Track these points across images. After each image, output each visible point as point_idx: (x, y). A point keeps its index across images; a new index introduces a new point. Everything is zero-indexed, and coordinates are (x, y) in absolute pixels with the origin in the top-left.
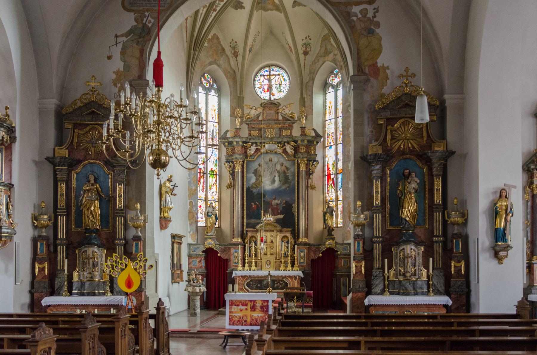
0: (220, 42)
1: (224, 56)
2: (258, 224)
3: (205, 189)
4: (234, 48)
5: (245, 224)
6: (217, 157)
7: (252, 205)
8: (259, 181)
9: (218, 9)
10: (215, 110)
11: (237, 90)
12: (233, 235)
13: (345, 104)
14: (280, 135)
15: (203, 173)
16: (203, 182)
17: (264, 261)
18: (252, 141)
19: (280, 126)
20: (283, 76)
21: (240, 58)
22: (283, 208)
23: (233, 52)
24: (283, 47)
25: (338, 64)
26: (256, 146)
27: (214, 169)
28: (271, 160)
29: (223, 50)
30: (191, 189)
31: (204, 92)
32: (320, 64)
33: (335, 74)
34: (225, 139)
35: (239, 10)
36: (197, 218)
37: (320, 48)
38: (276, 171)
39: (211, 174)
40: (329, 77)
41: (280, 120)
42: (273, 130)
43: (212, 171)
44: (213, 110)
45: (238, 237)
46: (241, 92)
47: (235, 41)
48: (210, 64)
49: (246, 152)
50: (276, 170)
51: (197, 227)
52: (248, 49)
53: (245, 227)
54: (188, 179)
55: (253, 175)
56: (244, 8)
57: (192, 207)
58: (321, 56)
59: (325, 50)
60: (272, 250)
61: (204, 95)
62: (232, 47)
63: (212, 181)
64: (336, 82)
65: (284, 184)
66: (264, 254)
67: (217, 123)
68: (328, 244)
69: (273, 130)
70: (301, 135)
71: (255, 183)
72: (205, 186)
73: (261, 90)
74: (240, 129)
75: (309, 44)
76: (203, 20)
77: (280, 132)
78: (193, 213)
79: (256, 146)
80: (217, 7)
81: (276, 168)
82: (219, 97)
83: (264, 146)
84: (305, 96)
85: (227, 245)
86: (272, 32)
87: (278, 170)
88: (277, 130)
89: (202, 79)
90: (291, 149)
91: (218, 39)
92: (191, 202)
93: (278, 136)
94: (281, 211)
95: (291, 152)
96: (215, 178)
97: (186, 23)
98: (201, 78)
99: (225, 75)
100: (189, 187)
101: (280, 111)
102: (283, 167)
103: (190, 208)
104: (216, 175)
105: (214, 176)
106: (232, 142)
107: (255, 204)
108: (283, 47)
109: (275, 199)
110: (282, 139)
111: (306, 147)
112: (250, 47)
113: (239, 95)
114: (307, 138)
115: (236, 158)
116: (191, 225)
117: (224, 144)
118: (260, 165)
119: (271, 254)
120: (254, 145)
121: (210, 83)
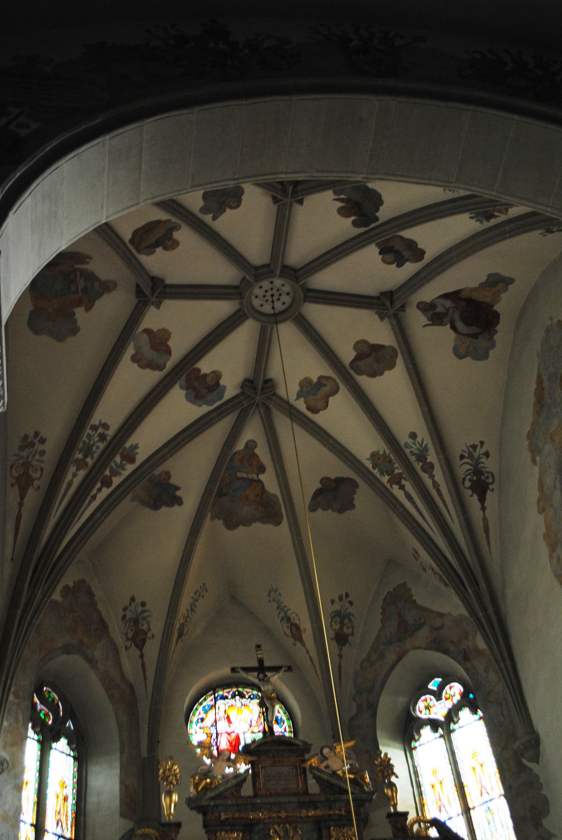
0: (96, 604)
9: (116, 481)
19: (319, 812)
23: (130, 635)
25: (452, 648)
29: (103, 626)
33: (432, 692)
35: (164, 509)
40: (416, 703)
42: (295, 829)
44: (61, 798)
47: (138, 600)
48: (67, 650)
56: (179, 501)
64: (445, 712)
69: (295, 829)
74: (178, 825)
75: (348, 616)
76: (66, 510)
80: (115, 473)
86: (234, 599)
91: (90, 594)
97: (21, 504)
99: (107, 690)
112: (182, 621)
113: (144, 753)
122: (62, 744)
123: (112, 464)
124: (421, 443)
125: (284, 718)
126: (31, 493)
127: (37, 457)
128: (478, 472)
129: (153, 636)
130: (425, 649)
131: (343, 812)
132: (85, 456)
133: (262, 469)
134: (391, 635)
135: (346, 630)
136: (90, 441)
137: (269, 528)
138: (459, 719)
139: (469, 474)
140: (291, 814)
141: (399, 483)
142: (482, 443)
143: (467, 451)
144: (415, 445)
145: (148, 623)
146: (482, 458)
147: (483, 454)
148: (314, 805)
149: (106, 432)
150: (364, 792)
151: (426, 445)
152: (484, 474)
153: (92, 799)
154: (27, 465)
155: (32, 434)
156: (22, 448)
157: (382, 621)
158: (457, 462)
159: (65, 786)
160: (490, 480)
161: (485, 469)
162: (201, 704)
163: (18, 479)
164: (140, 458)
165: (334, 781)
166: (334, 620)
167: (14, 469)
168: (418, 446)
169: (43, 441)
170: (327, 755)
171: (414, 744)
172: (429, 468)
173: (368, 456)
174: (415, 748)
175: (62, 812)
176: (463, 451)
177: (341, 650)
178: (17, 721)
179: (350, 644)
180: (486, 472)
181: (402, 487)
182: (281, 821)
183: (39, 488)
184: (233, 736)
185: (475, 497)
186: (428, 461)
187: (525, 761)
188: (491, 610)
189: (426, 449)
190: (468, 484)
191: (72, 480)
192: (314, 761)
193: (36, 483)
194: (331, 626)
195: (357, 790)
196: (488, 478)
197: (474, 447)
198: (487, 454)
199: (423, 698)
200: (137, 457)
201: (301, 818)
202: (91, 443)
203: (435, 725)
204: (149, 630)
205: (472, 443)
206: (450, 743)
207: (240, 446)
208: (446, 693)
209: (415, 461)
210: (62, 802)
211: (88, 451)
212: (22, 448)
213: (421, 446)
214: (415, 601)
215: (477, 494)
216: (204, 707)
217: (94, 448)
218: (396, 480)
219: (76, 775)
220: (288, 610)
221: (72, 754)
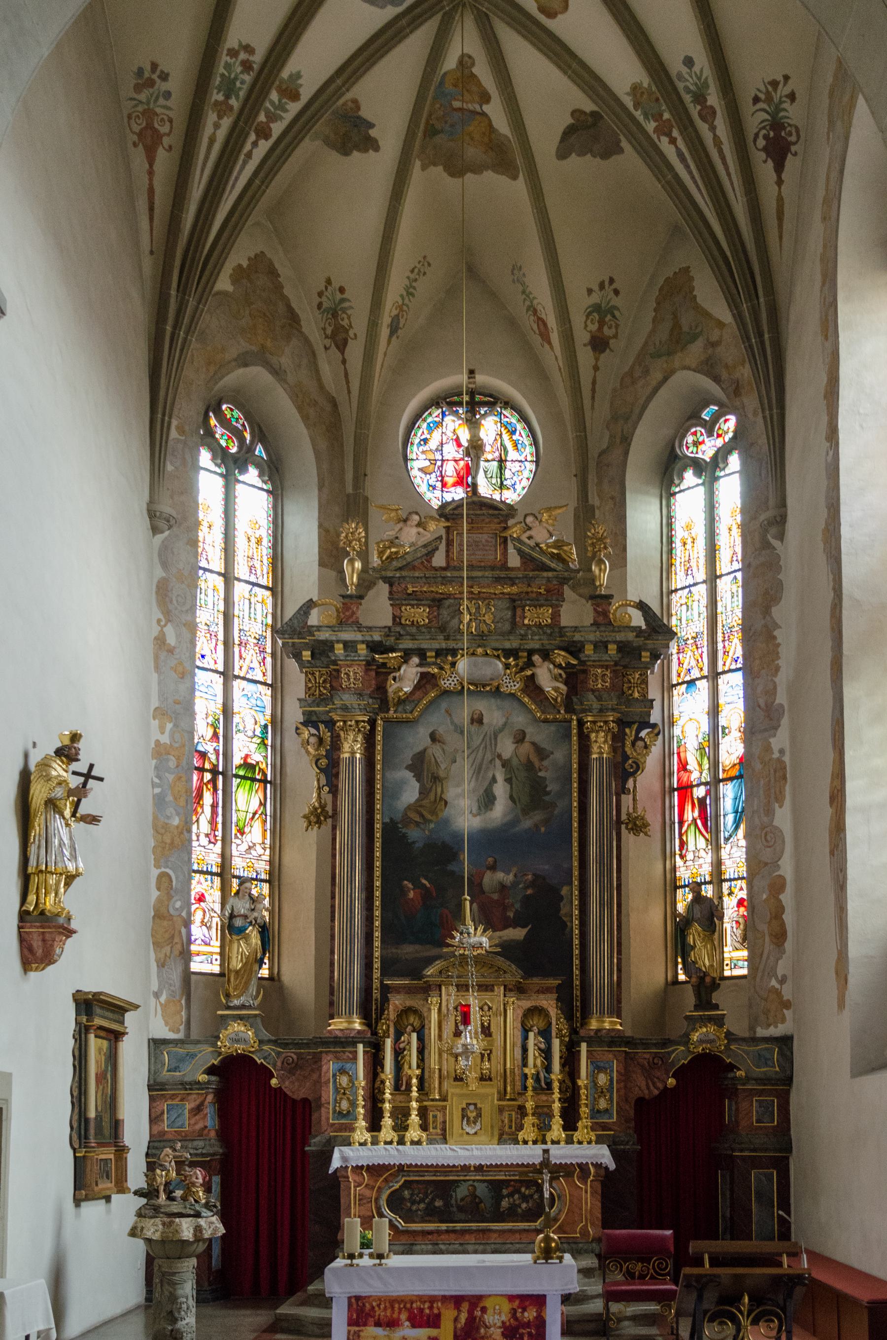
1: (294, 341)
2: (429, 961)
4: (335, 315)
5: (377, 965)
6: (269, 718)
7: (403, 892)
11: (343, 471)
12: (331, 1004)
14: (514, 624)
15: (214, 771)
17: (455, 1107)
19: (515, 589)
20: (513, 432)
21: (355, 351)
22: (526, 900)
23: (329, 331)
24: (512, 323)
26: (420, 665)
27: (256, 757)
31: (218, 470)
36: (190, 942)
39: (243, 778)
41: (512, 569)
43: (247, 765)
45: (351, 1013)
46: (360, 477)
51: (187, 975)
52: (386, 320)
53: (377, 974)
54: (154, 785)
61: (220, 482)
62: (327, 310)
65: (526, 811)
67: (266, 588)
70: (596, 624)
73: (433, 479)
77: (514, 616)
79: (420, 665)
82: (277, 493)
83: (453, 664)
84: (594, 499)
88: (505, 604)
89: (213, 422)
90: (556, 678)
92: (163, 876)
93: (507, 627)
94: (517, 913)
95: (556, 689)
96: (261, 794)
97: (151, 173)
98: (206, 418)
101: (515, 532)
105: (257, 785)
108: (512, 323)
110: (523, 637)
111: (614, 672)
113: (350, 490)
114: (620, 637)
116: (161, 965)
117: (297, 656)
119: (482, 1078)
120: (416, 660)
121: (241, 439)
122: (252, 475)
123: (267, 104)
124: (698, 73)
125: (527, 443)
126: (161, 154)
127: (161, 101)
128: (777, 125)
130: (695, 371)
131: (542, 591)
132: (227, 97)
133: (485, 98)
135: (607, 331)
136: (230, 74)
137: (503, 180)
139: (764, 128)
140: (484, 590)
141: (669, 134)
142: (786, 78)
143: (764, 90)
144: (691, 77)
145: (349, 318)
146: (785, 102)
147: (786, 96)
148: (512, 581)
149: (251, 58)
150: (568, 569)
151: (706, 78)
152: (785, 128)
154: (149, 114)
155: (148, 67)
156: (138, 88)
158: (747, 108)
159: (257, 526)
160: (793, 138)
161: (786, 120)
162: (424, 420)
163: (140, 135)
164: (306, 94)
166: (591, 317)
167: (133, 121)
168: (694, 78)
169: (164, 77)
172: (708, 114)
173: (628, 90)
174: (674, 494)
175: (255, 557)
176: (759, 90)
177: (597, 359)
179: (612, 350)
180: (790, 125)
181: (673, 141)
183: (170, 147)
185: (770, 164)
186: (709, 103)
189: (706, 85)
190: (761, 143)
191: (214, 133)
193: (166, 141)
194: (586, 326)
196: (790, 134)
197: (774, 84)
198: (792, 97)
200: (301, 90)
201: (495, 594)
202: (232, 76)
203: (698, 466)
205: (770, 79)
207: (450, 63)
208: (719, 428)
209: (692, 102)
210: (255, 545)
211: (229, 89)
212: (138, 88)
213: (699, 79)
214: (695, 297)
215: (773, 161)
216: (429, 424)
217: (238, 84)
218: (664, 130)
219: (271, 513)
220: (534, 298)
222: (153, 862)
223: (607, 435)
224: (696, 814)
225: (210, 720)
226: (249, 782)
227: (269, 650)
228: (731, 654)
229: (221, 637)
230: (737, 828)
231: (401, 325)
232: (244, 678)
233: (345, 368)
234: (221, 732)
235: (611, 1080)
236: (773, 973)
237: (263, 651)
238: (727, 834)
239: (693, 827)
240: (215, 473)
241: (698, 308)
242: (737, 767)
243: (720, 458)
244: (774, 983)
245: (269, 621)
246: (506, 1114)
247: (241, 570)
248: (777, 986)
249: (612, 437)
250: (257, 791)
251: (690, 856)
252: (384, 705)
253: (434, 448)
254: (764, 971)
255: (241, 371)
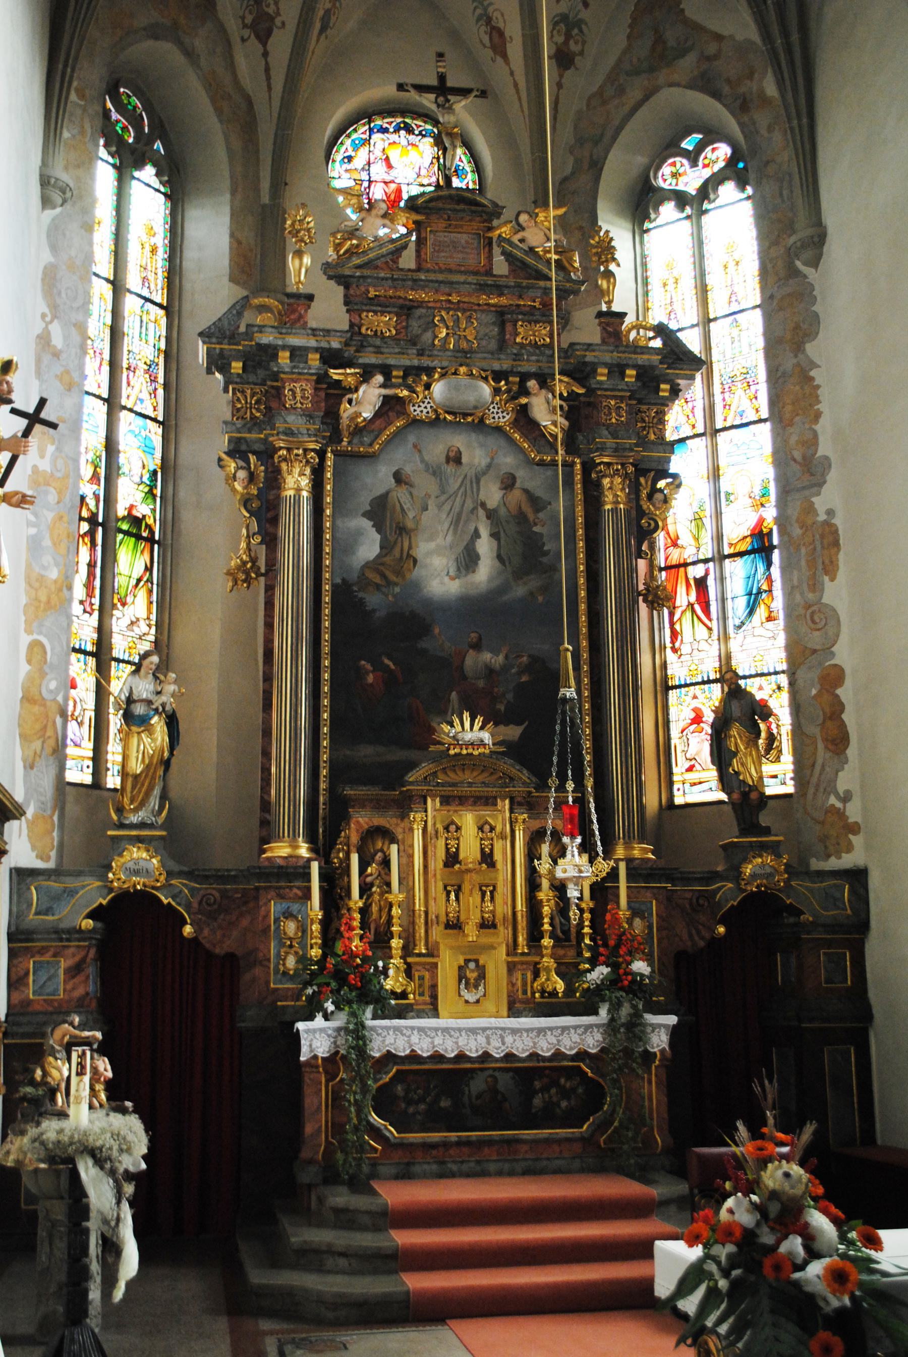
3: (96, 601)
6: (159, 462)
8: (397, 552)
10: (154, 251)
11: (257, 179)
13: (776, 243)
15: (92, 520)
16: (91, 565)
18: (369, 358)
19: (503, 301)
23: (249, 19)
25: (726, 90)
27: (143, 510)
28: (456, 459)
30: (41, 579)
32: (631, 103)
33: (686, 154)
34: (233, 338)
37: (625, 44)
38: (481, 513)
39: (127, 533)
40: (659, 167)
44: (148, 248)
46: (279, 185)
49: (331, 416)
50: (483, 505)
55: (367, 524)
57: (43, 674)
58: (637, 72)
59: (653, 49)
60: (489, 906)
63: (132, 565)
64: (698, 183)
66: (448, 926)
67: (160, 306)
68: (754, 876)
71: (375, 565)
72: (97, 583)
74: (310, 298)
77: (502, 331)
78: (43, 702)
79: (383, 386)
81: (482, 497)
83: (428, 387)
85: (234, 879)
87: (492, 503)
88: (490, 318)
92: (35, 647)
93: (493, 345)
99: (213, 101)
100: (29, 566)
102: (516, 495)
103: (29, 678)
104: (151, 540)
106: (271, 352)
107: (378, 666)
109: (477, 646)
110: (517, 357)
113: (266, 199)
115: (289, 433)
118: (398, 478)
120: (379, 379)
122: (148, 173)
125: (468, 169)
129: (283, 24)
130: (685, 87)
131: (537, 304)
134: (639, 59)
135: (573, 47)
138: (718, 196)
140: (466, 300)
148: (498, 289)
150: (570, 280)
153: (190, 255)
157: (629, 37)
159: (152, 233)
162: (348, 136)
165: (530, 260)
166: (557, 28)
170: (524, 225)
171: (647, 225)
174: (648, 231)
175: (149, 268)
177: (561, 76)
178: (82, 132)
179: (577, 69)
182: (450, 307)
184: (393, 186)
187: (798, 264)
188: (795, 37)
192: (505, 231)
195: (562, 274)
199: (671, 161)
201: (479, 305)
203: (681, 199)
204: (278, 14)
206: (699, 227)
208: (706, 158)
210: (149, 254)
214: (683, 11)
216: (353, 141)
219: (169, 220)
221: (162, 189)
222: (23, 626)
223: (571, 160)
224: (693, 597)
225: (91, 456)
226: (133, 539)
227: (161, 380)
228: (733, 408)
229: (107, 356)
230: (751, 613)
231: (331, 25)
232: (131, 410)
233: (267, 63)
234: (102, 472)
235: (650, 927)
236: (831, 788)
237: (154, 380)
238: (738, 623)
239: (688, 614)
240: (107, 162)
241: (687, 23)
242: (749, 539)
243: (706, 191)
244: (833, 800)
245: (163, 346)
246: (518, 975)
247: (133, 281)
248: (839, 805)
249: (578, 162)
250: (142, 552)
251: (685, 649)
252: (335, 436)
253: (360, 167)
254: (817, 786)
255: (150, 43)
